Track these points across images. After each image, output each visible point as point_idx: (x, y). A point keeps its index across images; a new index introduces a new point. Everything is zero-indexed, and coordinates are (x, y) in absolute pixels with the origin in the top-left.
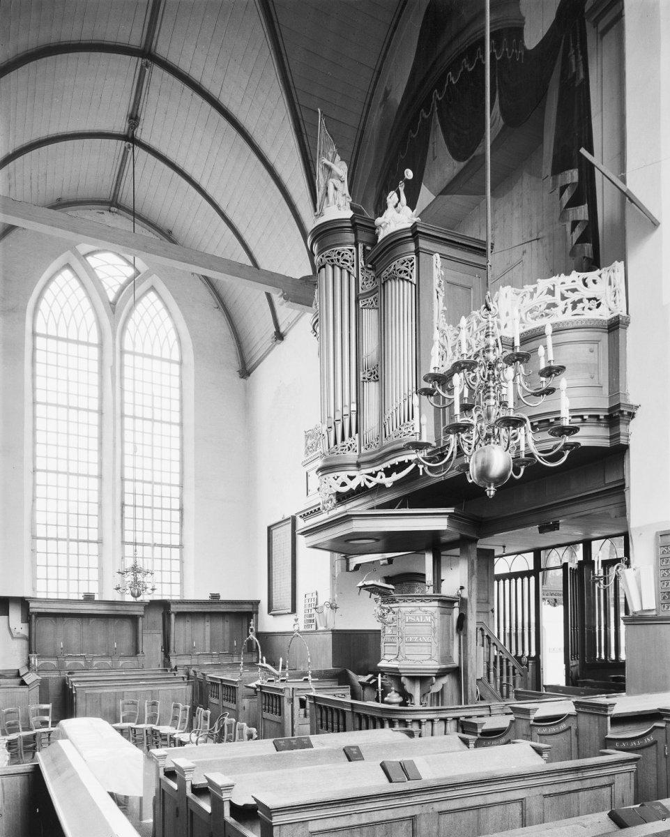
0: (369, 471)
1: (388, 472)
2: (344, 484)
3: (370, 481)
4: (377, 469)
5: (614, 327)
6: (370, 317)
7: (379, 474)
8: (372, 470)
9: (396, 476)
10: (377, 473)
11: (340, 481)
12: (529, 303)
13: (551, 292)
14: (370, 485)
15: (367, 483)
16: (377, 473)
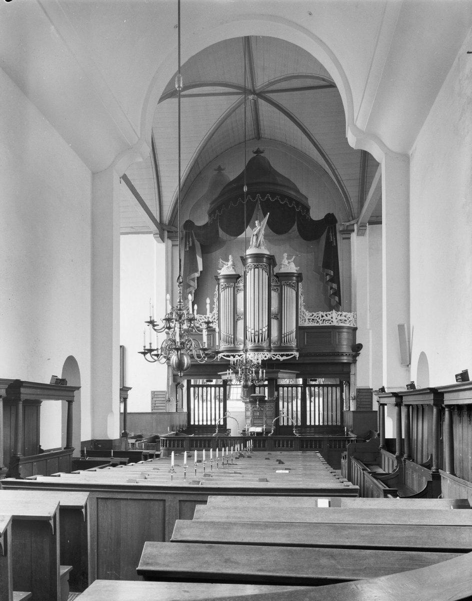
0: (274, 353)
1: (282, 356)
2: (266, 357)
3: (274, 357)
4: (277, 353)
5: (355, 329)
6: (274, 295)
7: (278, 355)
8: (275, 353)
9: (285, 358)
10: (277, 355)
11: (265, 355)
12: (339, 318)
13: (345, 316)
14: (274, 359)
15: (272, 358)
16: (277, 355)
